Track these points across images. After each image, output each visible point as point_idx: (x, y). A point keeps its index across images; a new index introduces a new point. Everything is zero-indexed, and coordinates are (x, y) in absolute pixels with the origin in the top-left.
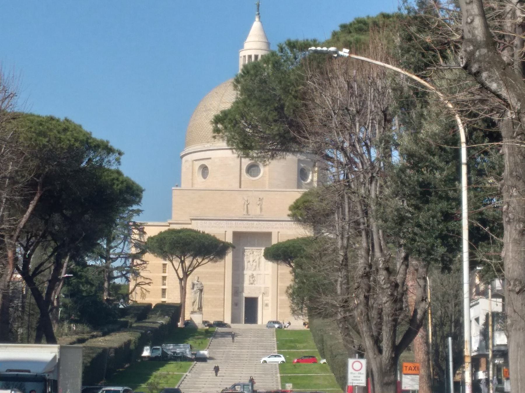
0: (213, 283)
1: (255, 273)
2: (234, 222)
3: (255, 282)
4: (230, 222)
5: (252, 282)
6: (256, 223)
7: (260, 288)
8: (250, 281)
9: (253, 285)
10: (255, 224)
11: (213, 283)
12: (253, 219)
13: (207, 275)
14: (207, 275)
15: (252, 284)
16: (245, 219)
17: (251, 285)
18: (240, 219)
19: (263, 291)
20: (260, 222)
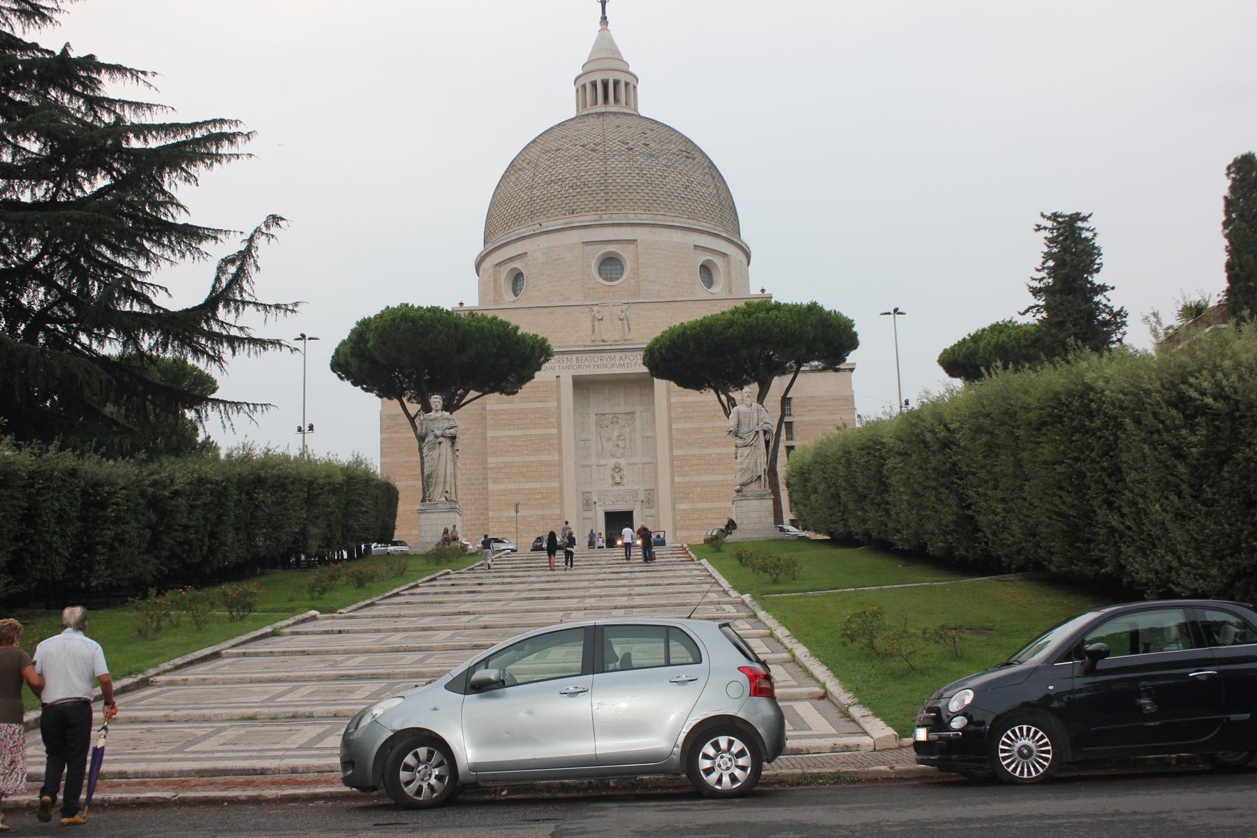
1: (622, 461)
2: (574, 357)
3: (625, 481)
4: (565, 356)
5: (618, 479)
6: (618, 355)
7: (635, 492)
9: (621, 487)
10: (618, 358)
12: (613, 347)
13: (524, 469)
14: (524, 469)
15: (617, 484)
16: (595, 348)
17: (616, 488)
18: (586, 348)
19: (642, 497)
20: (628, 354)
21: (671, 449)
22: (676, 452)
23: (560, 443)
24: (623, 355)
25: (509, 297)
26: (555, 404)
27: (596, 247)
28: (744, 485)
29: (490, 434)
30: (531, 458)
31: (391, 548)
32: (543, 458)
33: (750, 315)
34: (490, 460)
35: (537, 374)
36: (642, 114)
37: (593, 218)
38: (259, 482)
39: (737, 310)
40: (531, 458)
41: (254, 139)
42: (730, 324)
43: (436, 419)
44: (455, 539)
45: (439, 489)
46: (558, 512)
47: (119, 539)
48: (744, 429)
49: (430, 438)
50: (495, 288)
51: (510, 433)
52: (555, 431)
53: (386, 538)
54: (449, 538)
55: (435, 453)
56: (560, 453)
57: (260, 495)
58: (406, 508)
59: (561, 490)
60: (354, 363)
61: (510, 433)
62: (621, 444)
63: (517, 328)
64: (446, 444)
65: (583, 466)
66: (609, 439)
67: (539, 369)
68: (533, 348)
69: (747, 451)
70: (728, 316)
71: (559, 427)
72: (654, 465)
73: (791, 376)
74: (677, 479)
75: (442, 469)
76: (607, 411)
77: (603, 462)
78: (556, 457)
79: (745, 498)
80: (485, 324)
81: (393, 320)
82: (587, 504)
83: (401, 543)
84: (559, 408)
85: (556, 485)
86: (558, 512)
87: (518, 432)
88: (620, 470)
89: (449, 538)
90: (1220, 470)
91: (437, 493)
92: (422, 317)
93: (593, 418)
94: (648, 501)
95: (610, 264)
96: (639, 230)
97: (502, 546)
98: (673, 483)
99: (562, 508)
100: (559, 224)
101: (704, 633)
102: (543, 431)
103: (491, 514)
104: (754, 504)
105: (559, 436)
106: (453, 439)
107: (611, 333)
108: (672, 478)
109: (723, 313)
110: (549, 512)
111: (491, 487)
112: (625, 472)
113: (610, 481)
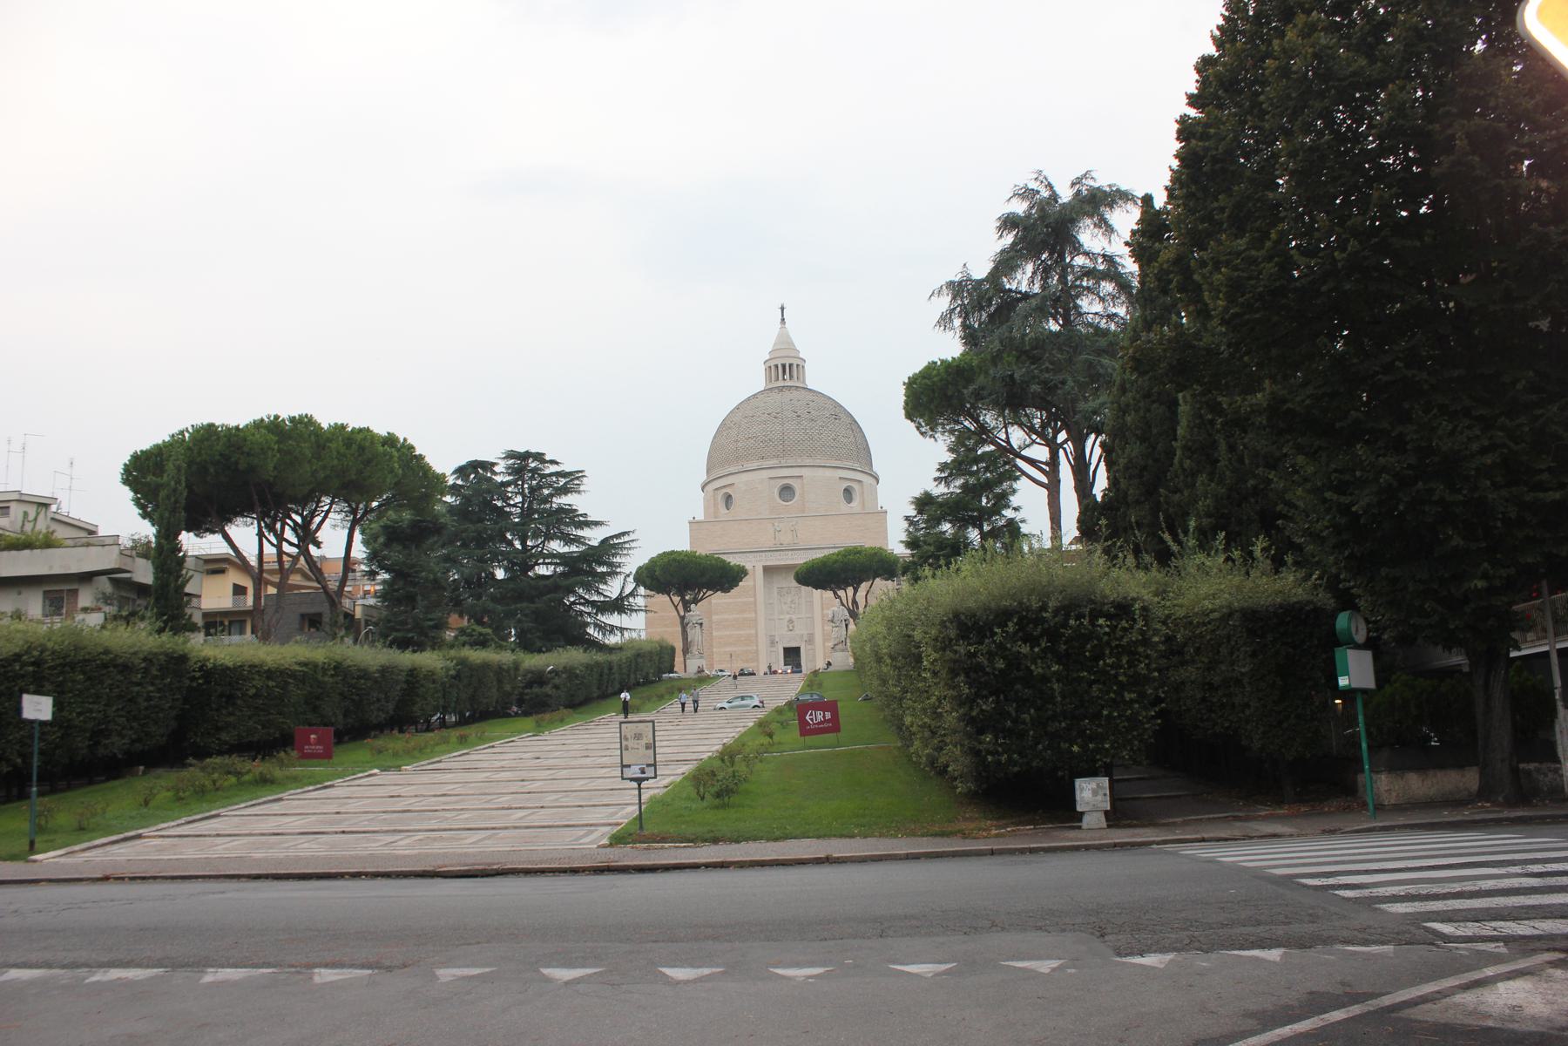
0: (742, 632)
4: (758, 554)
5: (791, 628)
8: (788, 627)
9: (792, 632)
11: (742, 632)
17: (790, 633)
21: (822, 609)
22: (825, 612)
23: (756, 606)
24: (792, 552)
25: (723, 510)
26: (751, 583)
27: (779, 480)
28: (835, 645)
29: (713, 601)
30: (738, 616)
31: (671, 675)
32: (745, 616)
33: (845, 556)
34: (715, 618)
35: (740, 583)
36: (811, 383)
37: (777, 462)
38: (638, 655)
39: (839, 553)
40: (738, 616)
41: (636, 532)
42: (836, 561)
43: (692, 616)
44: (703, 671)
45: (695, 648)
46: (755, 648)
47: (614, 679)
48: (836, 619)
49: (691, 624)
50: (715, 504)
51: (726, 601)
52: (752, 599)
53: (672, 671)
54: (700, 671)
55: (694, 631)
56: (756, 613)
57: (640, 660)
58: (679, 659)
59: (757, 634)
60: (648, 582)
61: (726, 601)
62: (793, 606)
63: (729, 563)
64: (698, 627)
65: (770, 620)
66: (785, 603)
67: (741, 581)
68: (738, 572)
69: (837, 629)
70: (835, 557)
71: (755, 596)
72: (813, 618)
73: (870, 582)
74: (826, 628)
75: (696, 638)
76: (784, 586)
77: (782, 617)
78: (754, 615)
79: (836, 651)
80: (713, 562)
81: (669, 561)
82: (773, 643)
83: (676, 672)
84: (755, 586)
85: (753, 632)
86: (755, 648)
87: (731, 600)
88: (793, 622)
89: (700, 671)
90: (1006, 649)
91: (694, 650)
92: (683, 560)
93: (775, 590)
94: (810, 641)
95: (787, 491)
96: (804, 470)
97: (724, 674)
98: (824, 630)
99: (757, 646)
100: (755, 465)
101: (755, 696)
102: (745, 600)
103: (715, 650)
104: (840, 654)
105: (755, 603)
106: (701, 624)
107: (786, 539)
108: (823, 627)
109: (833, 554)
110: (750, 648)
111: (715, 634)
112: (795, 623)
113: (786, 629)
